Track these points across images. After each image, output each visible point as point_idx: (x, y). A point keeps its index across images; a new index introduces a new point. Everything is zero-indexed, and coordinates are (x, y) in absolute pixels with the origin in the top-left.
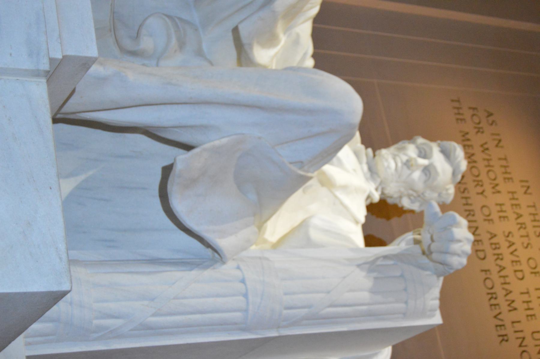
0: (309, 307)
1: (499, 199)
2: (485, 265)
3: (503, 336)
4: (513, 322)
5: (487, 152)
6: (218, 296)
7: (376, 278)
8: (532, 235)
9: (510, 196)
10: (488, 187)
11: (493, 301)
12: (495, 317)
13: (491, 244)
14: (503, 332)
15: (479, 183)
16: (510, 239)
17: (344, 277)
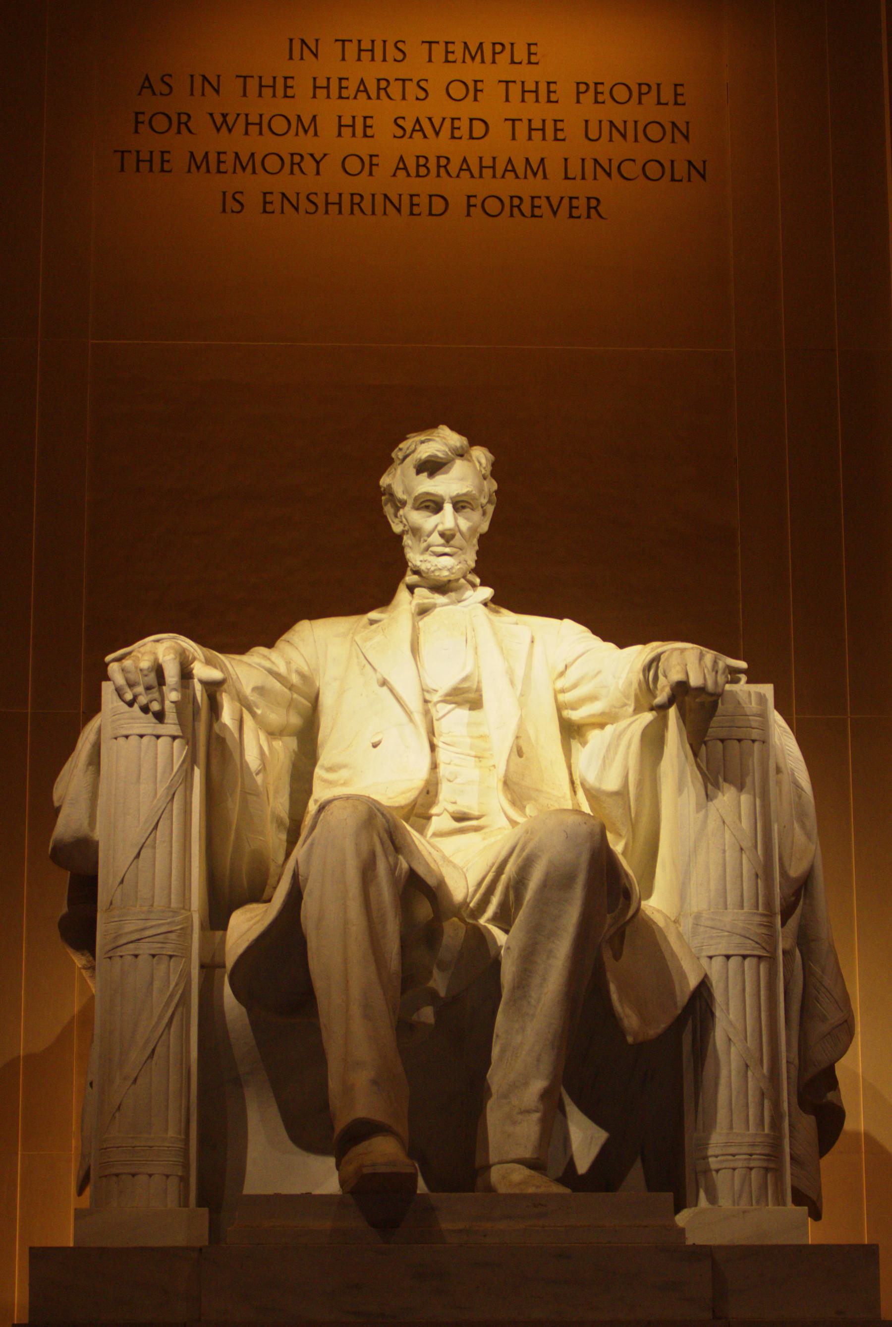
0: (757, 876)
1: (328, 126)
2: (458, 204)
3: (589, 208)
4: (566, 178)
5: (230, 120)
6: (744, 990)
7: (725, 780)
8: (401, 70)
9: (321, 93)
10: (305, 144)
11: (526, 207)
12: (555, 213)
13: (418, 176)
14: (582, 203)
15: (296, 162)
16: (409, 127)
17: (724, 822)
